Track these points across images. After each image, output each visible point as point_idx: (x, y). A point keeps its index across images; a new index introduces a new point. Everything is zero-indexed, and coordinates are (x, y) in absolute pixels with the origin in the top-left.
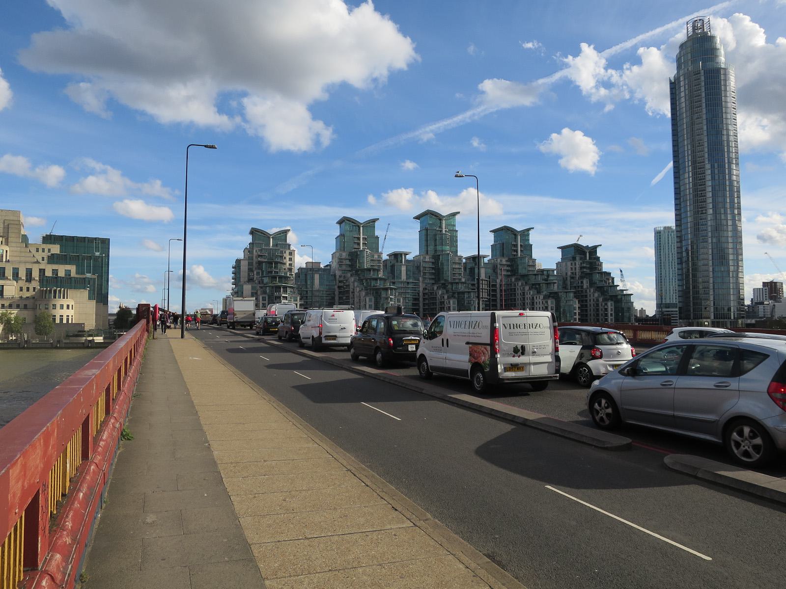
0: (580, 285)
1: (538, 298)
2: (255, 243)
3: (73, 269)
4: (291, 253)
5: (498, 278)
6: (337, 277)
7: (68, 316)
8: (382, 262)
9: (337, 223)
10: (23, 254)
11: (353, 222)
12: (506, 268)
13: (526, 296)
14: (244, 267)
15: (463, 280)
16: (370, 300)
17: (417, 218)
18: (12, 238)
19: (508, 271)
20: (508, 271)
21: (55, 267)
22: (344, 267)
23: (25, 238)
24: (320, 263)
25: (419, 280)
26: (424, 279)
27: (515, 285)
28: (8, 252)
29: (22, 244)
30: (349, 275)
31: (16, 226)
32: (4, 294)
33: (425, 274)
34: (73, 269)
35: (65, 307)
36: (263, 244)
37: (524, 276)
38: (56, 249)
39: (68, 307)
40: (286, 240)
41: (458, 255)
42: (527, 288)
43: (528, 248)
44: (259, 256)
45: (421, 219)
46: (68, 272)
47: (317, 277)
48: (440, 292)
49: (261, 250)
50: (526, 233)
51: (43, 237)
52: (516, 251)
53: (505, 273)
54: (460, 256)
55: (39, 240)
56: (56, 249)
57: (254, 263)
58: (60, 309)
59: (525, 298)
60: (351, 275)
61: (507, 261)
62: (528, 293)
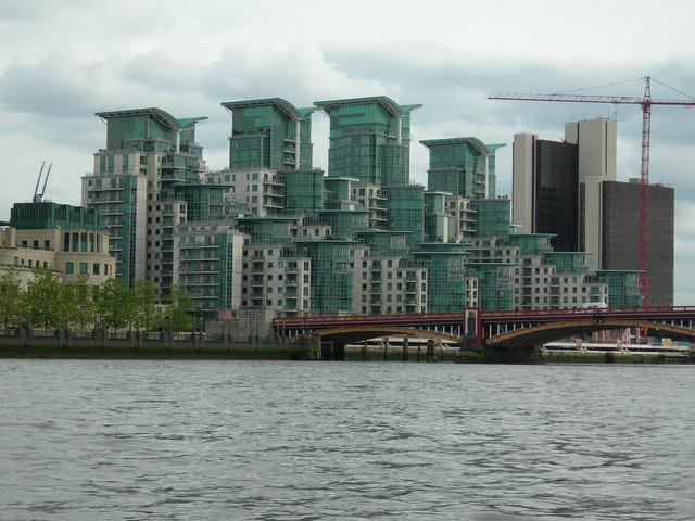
1: (570, 280)
13: (534, 276)
42: (536, 262)
53: (465, 229)
59: (530, 279)
62: (542, 271)
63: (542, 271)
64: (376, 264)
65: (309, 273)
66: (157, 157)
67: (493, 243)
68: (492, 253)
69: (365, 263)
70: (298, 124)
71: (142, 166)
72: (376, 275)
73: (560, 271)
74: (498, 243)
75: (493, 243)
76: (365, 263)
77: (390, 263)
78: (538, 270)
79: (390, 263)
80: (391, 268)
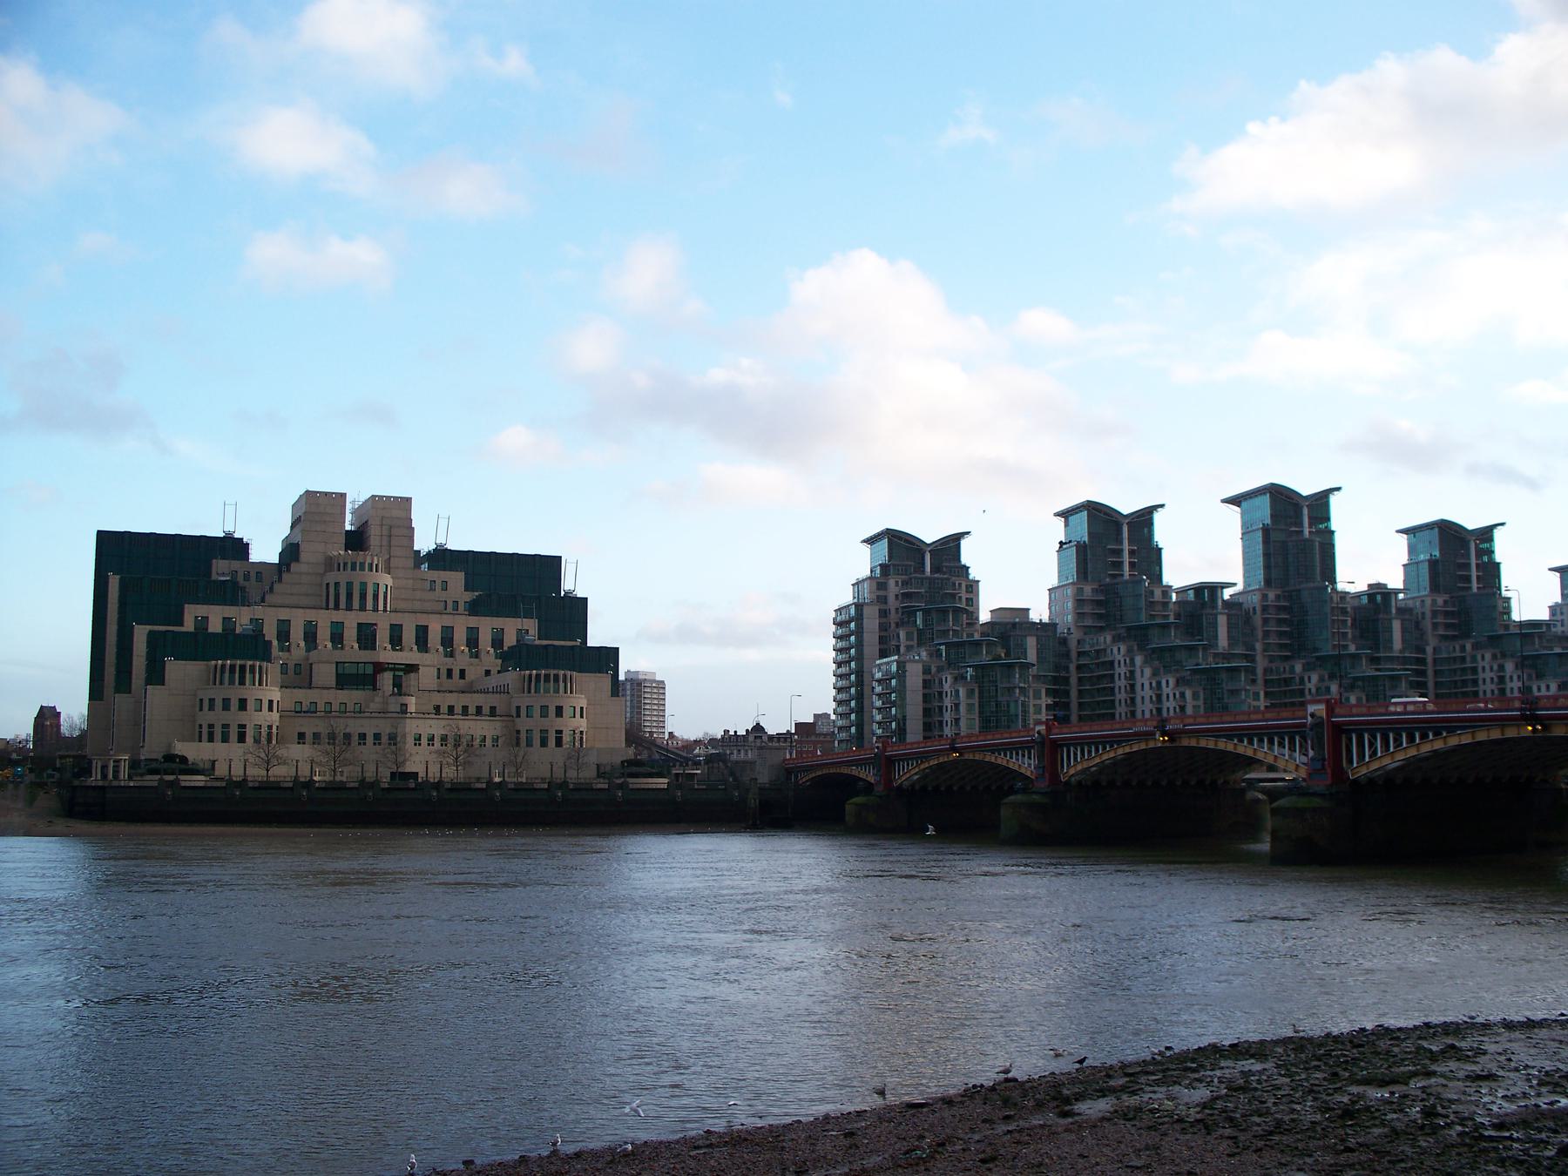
0: (1458, 654)
2: (894, 565)
3: (531, 625)
4: (971, 586)
5: (1428, 645)
6: (1073, 644)
8: (1171, 606)
9: (1058, 514)
11: (1105, 514)
12: (1440, 620)
14: (872, 623)
15: (1352, 649)
16: (1195, 696)
17: (1235, 501)
19: (1447, 626)
20: (1447, 626)
22: (1089, 622)
24: (1029, 609)
25: (1254, 649)
26: (1266, 648)
27: (1474, 659)
30: (1109, 638)
33: (1266, 634)
34: (531, 625)
36: (911, 566)
37: (1494, 640)
40: (960, 561)
41: (1164, 583)
42: (1509, 667)
43: (1491, 571)
44: (907, 596)
45: (1244, 504)
46: (521, 633)
47: (1031, 643)
48: (1315, 678)
49: (905, 583)
50: (1486, 534)
52: (1468, 579)
54: (1342, 592)
57: (893, 611)
60: (1114, 637)
61: (1278, 597)
62: (1515, 678)
63: (1515, 678)
64: (1159, 683)
65: (976, 701)
66: (892, 583)
67: (1468, 647)
68: (1468, 659)
69: (1151, 684)
70: (1125, 529)
71: (881, 593)
72: (1159, 697)
73: (1540, 676)
74: (1476, 646)
75: (1468, 647)
76: (1151, 684)
77: (1167, 681)
78: (1511, 678)
79: (1167, 681)
80: (1169, 685)
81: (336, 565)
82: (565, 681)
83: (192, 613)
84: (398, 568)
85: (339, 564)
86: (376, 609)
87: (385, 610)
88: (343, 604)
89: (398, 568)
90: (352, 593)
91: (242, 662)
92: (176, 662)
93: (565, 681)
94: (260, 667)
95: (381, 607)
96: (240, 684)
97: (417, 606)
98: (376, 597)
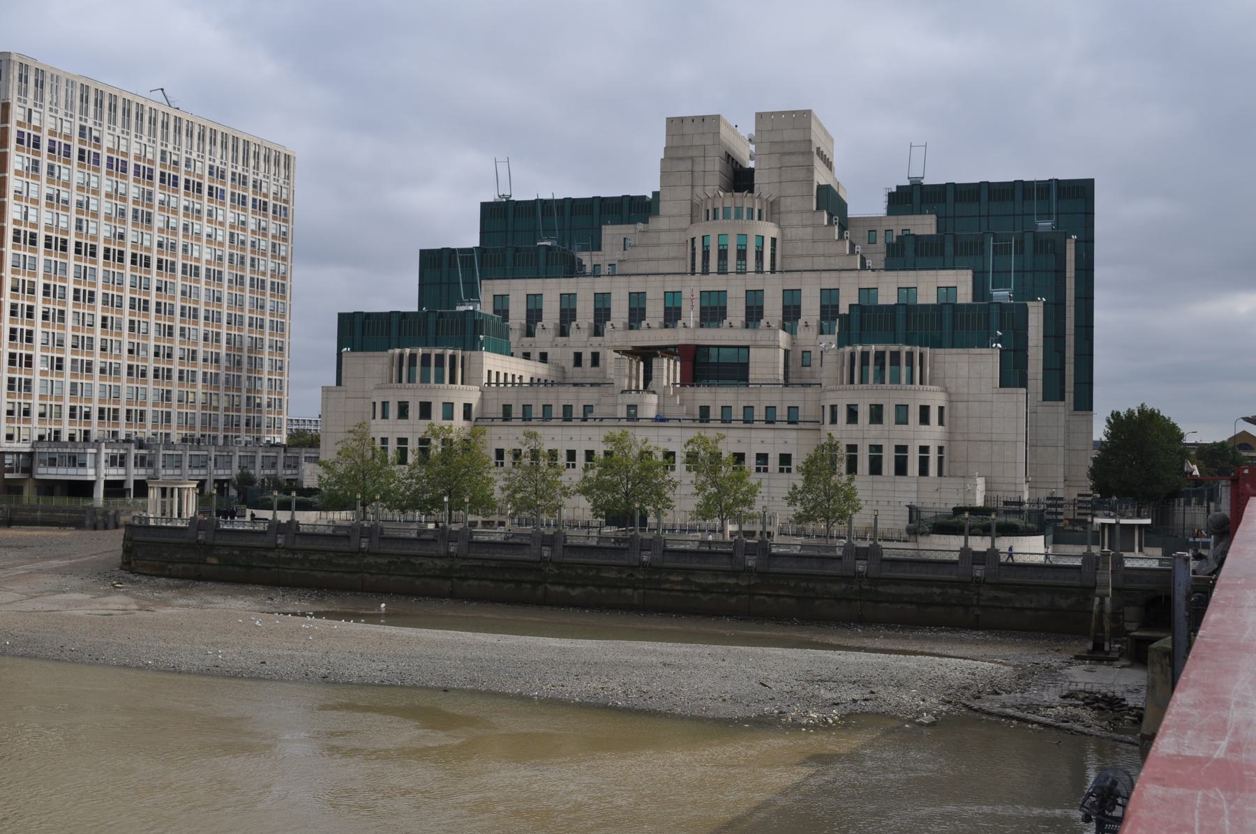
7: (924, 449)
10: (821, 248)
18: (789, 200)
21: (907, 278)
23: (829, 200)
28: (778, 243)
29: (818, 213)
31: (800, 160)
32: (751, 376)
35: (842, 415)
38: (924, 225)
39: (852, 415)
51: (891, 195)
55: (879, 208)
56: (924, 225)
58: (898, 422)
81: (704, 213)
82: (910, 363)
83: (490, 289)
84: (791, 212)
85: (708, 211)
86: (759, 270)
87: (773, 271)
88: (699, 268)
89: (791, 212)
90: (708, 251)
91: (439, 351)
92: (354, 354)
93: (910, 363)
94: (453, 358)
95: (767, 266)
96: (422, 381)
97: (820, 263)
98: (759, 256)
